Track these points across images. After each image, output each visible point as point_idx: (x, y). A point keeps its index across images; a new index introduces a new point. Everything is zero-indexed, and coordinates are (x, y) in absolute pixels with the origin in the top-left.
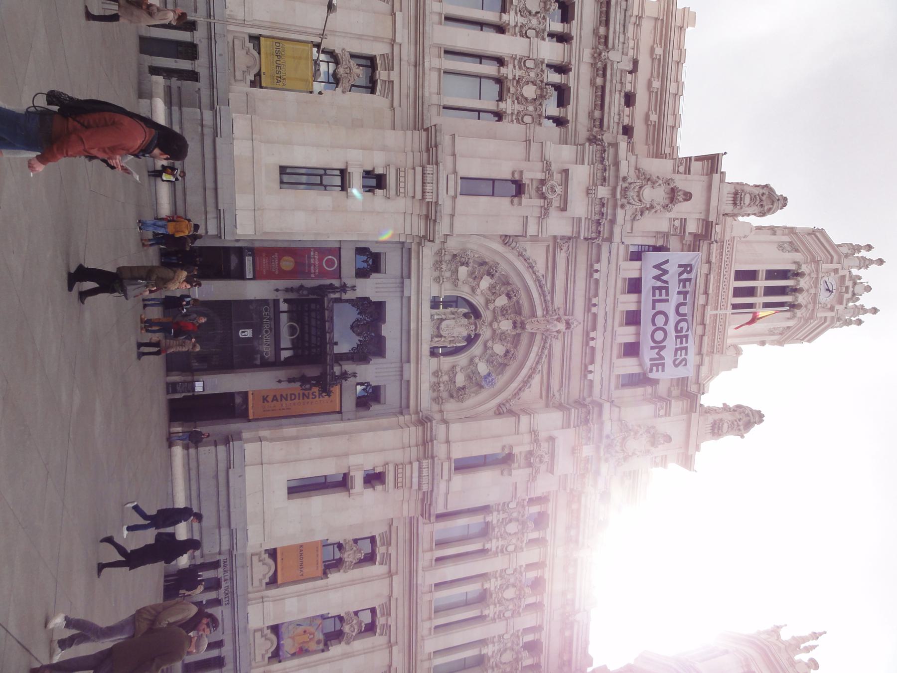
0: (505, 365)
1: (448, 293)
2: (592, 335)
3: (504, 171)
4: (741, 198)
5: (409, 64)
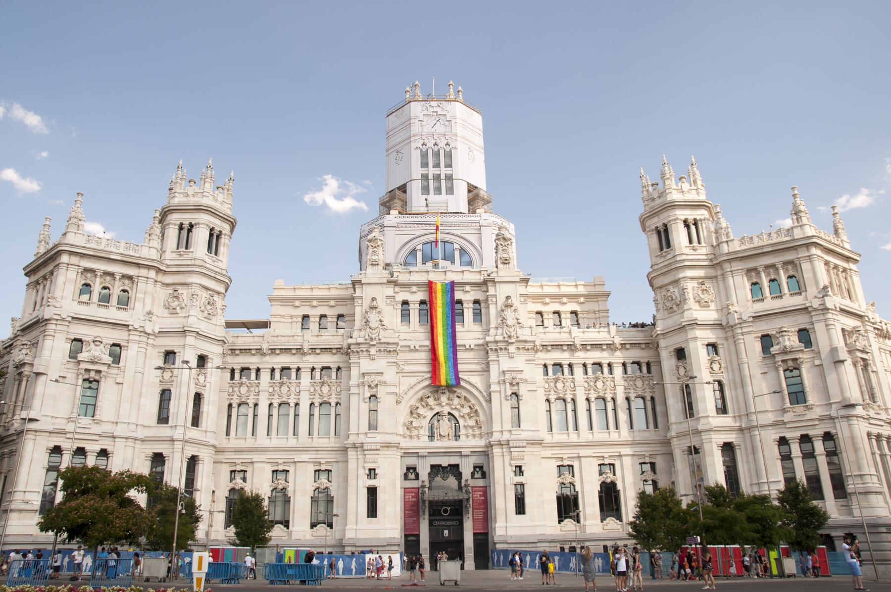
0: (465, 398)
1: (427, 431)
5: (317, 454)
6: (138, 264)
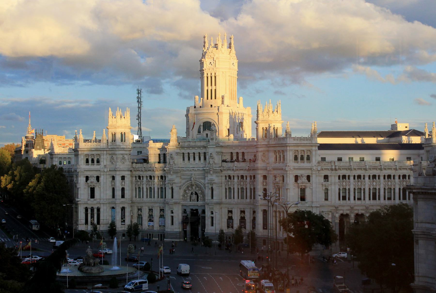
0: (200, 187)
3: (170, 191)
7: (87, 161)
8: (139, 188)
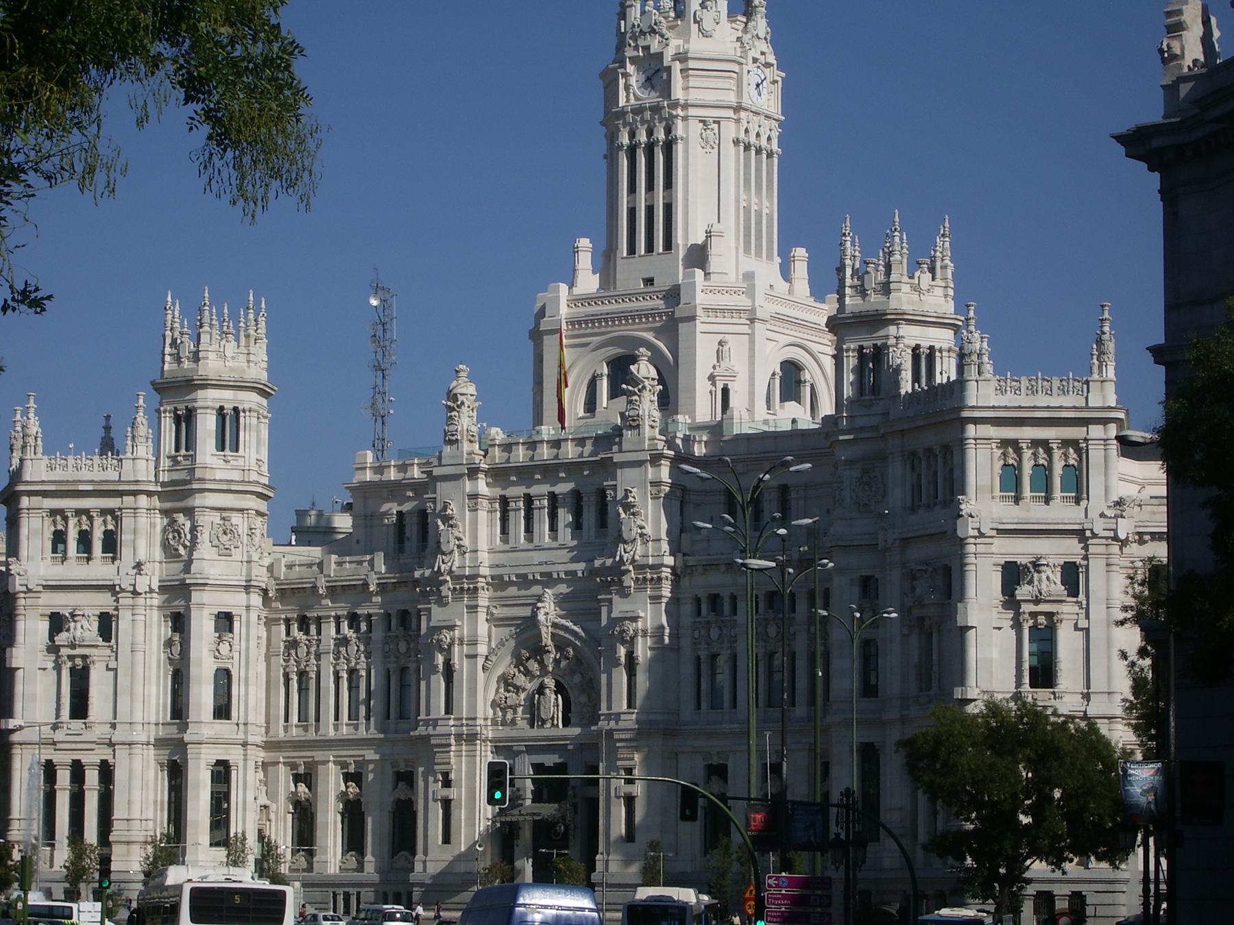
2: (555, 576)
4: (452, 435)
6: (118, 490)
7: (59, 538)
8: (302, 674)
